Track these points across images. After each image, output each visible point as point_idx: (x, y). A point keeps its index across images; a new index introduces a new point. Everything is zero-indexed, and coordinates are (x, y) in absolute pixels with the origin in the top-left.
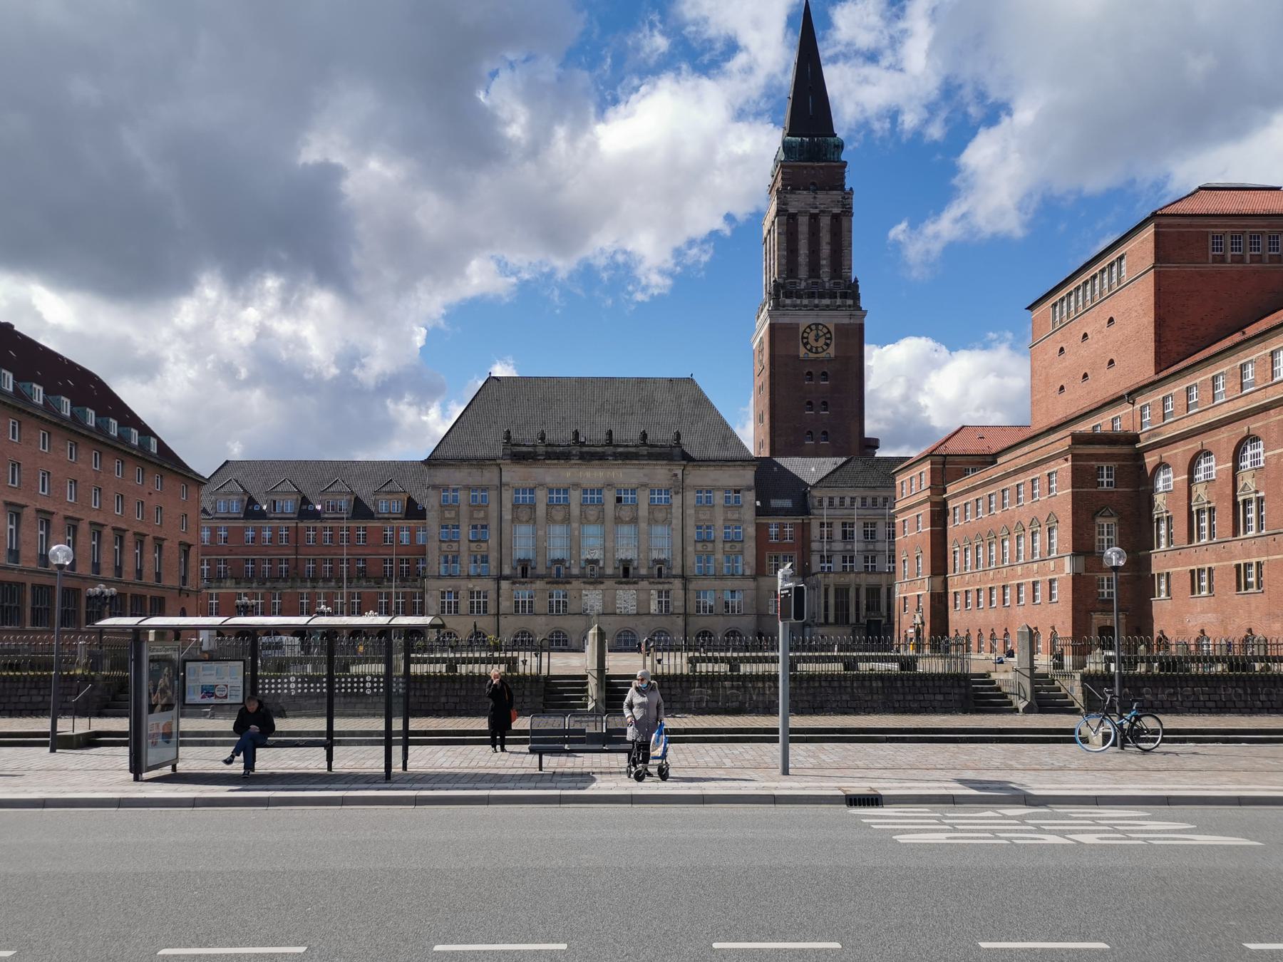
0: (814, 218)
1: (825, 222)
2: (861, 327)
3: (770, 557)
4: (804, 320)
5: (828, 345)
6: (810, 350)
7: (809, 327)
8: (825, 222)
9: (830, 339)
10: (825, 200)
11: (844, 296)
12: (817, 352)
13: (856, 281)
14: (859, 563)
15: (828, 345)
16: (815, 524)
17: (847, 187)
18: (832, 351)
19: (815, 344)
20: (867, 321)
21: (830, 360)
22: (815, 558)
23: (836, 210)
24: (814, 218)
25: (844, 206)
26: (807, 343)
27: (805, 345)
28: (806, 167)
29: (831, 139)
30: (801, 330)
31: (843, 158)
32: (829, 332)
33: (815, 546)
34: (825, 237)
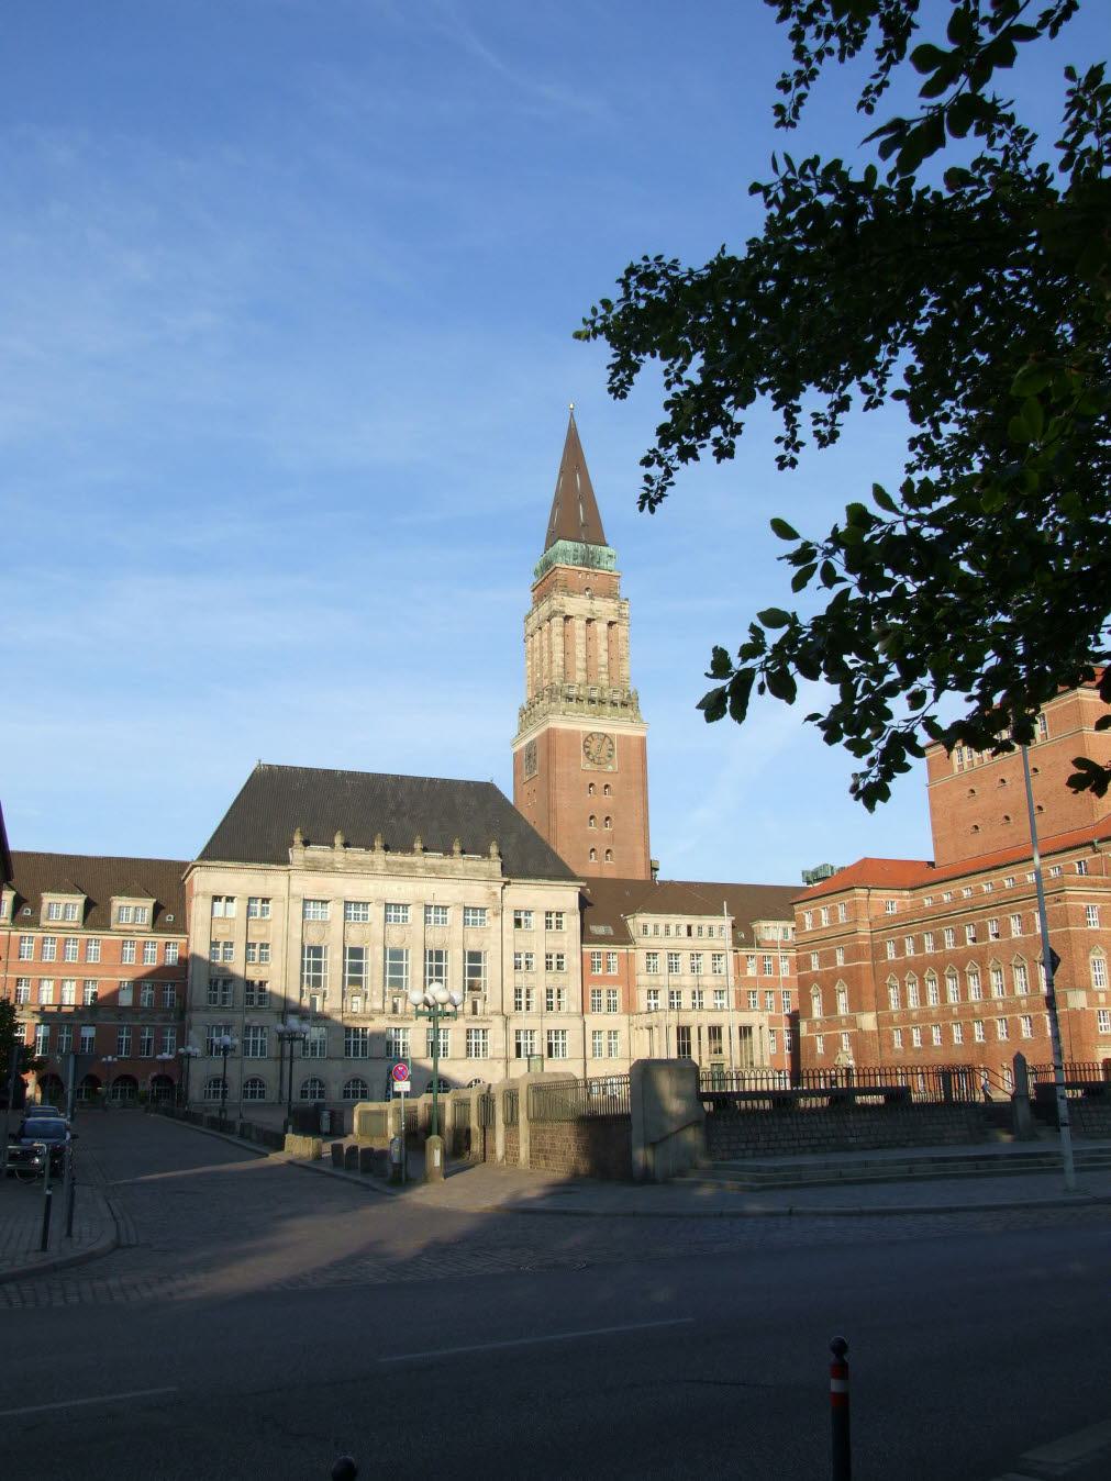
1: (601, 627)
2: (643, 740)
3: (594, 991)
5: (610, 756)
7: (591, 735)
10: (604, 608)
11: (624, 704)
14: (686, 1001)
16: (641, 956)
22: (642, 995)
23: (613, 618)
25: (620, 615)
26: (588, 753)
28: (580, 572)
29: (604, 549)
32: (611, 743)
33: (643, 979)
34: (603, 645)
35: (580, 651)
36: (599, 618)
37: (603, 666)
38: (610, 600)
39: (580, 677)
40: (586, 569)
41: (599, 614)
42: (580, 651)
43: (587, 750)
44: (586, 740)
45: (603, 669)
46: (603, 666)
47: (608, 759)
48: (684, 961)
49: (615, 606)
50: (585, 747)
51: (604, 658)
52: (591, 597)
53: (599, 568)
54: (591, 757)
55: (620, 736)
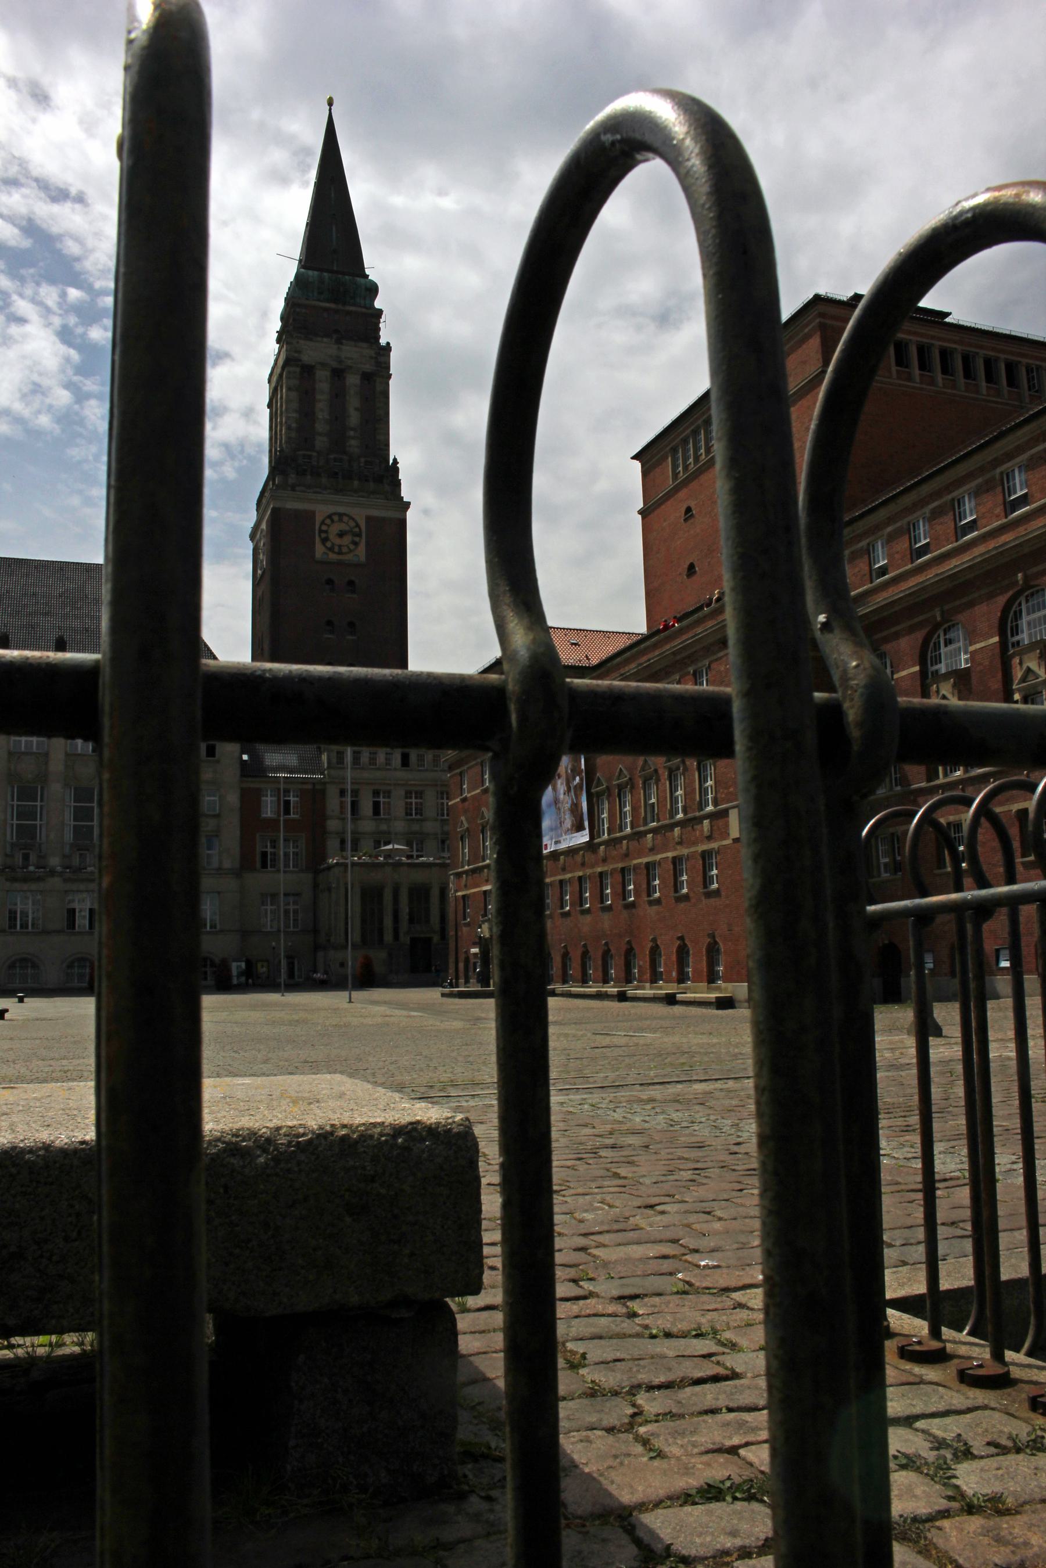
0: (338, 374)
1: (353, 380)
2: (402, 524)
4: (322, 507)
5: (356, 544)
6: (331, 549)
7: (330, 517)
8: (353, 380)
9: (359, 535)
11: (379, 480)
12: (340, 553)
13: (395, 460)
15: (356, 544)
17: (383, 341)
18: (361, 552)
19: (338, 541)
20: (412, 517)
21: (358, 565)
23: (368, 367)
24: (338, 374)
27: (324, 541)
28: (326, 310)
30: (319, 519)
31: (378, 304)
32: (357, 525)
34: (353, 403)
35: (322, 410)
36: (351, 367)
37: (352, 429)
38: (365, 345)
39: (321, 442)
40: (332, 306)
41: (349, 362)
42: (322, 410)
43: (323, 535)
44: (323, 523)
45: (352, 433)
46: (352, 429)
47: (352, 547)
48: (398, 804)
49: (372, 353)
50: (321, 531)
51: (354, 418)
52: (339, 342)
53: (354, 305)
54: (329, 544)
55: (369, 519)
